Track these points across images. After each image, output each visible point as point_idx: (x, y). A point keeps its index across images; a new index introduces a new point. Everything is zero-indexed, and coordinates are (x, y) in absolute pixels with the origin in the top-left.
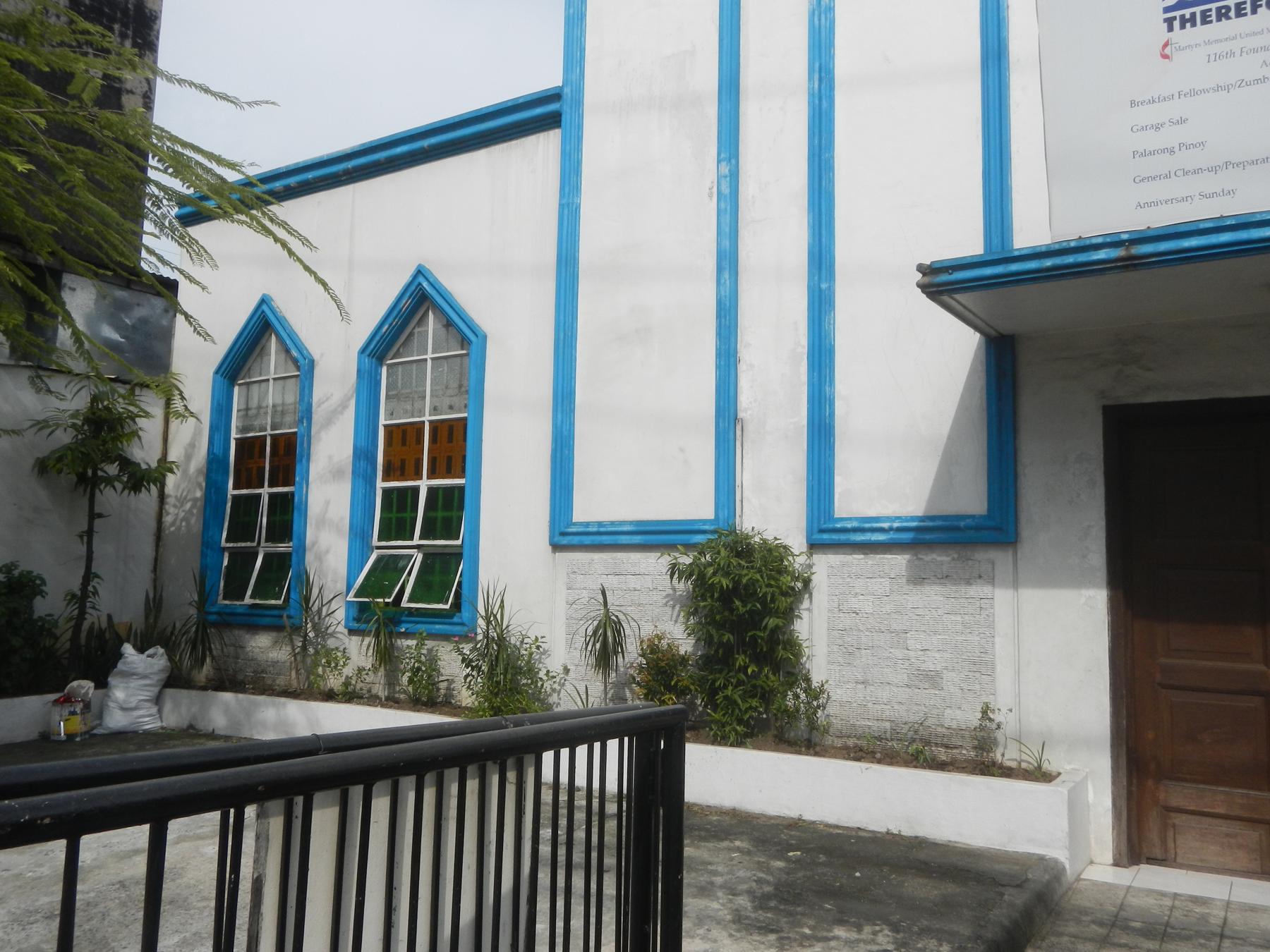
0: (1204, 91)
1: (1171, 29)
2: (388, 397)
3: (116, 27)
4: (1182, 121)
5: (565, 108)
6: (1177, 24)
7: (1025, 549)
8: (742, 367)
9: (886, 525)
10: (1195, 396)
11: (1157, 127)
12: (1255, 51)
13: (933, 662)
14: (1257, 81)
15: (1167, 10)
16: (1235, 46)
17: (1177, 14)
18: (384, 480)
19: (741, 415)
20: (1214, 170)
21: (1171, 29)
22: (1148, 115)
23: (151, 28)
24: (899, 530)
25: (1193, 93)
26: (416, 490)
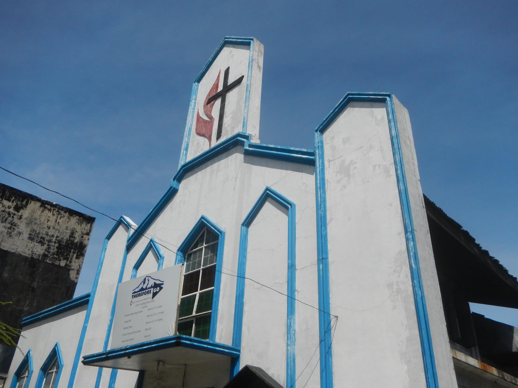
3: (72, 250)
4: (130, 321)
5: (90, 298)
8: (102, 377)
11: (127, 322)
15: (133, 293)
16: (139, 303)
20: (132, 333)
22: (128, 318)
25: (133, 314)
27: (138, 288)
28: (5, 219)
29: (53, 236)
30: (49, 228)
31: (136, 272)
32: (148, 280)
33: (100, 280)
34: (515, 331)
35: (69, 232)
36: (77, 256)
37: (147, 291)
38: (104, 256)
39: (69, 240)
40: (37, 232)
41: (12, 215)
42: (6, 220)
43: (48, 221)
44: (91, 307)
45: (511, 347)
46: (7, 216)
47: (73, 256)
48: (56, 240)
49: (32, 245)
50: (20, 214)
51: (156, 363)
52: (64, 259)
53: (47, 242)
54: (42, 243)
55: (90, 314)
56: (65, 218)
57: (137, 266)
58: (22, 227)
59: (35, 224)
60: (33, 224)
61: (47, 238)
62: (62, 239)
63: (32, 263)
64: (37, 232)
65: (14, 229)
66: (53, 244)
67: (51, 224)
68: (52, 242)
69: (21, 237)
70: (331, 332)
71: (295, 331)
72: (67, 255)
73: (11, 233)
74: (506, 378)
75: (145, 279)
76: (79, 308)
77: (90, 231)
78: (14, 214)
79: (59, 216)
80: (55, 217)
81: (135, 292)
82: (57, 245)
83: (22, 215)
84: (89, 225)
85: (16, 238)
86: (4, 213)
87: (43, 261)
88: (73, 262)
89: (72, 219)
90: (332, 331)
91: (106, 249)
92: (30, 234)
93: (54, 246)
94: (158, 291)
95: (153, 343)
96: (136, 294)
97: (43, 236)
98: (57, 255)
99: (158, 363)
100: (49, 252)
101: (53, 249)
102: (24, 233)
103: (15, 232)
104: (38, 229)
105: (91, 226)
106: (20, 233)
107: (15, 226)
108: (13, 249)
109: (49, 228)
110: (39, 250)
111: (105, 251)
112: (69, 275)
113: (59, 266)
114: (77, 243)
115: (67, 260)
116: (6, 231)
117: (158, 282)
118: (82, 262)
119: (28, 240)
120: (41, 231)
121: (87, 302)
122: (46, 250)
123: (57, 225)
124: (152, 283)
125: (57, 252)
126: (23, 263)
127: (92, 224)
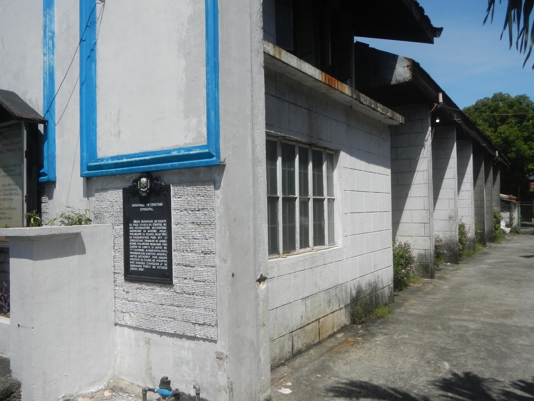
34: (399, 60)
45: (391, 79)
70: (95, 26)
71: (54, 33)
74: (362, 100)
90: (98, 25)
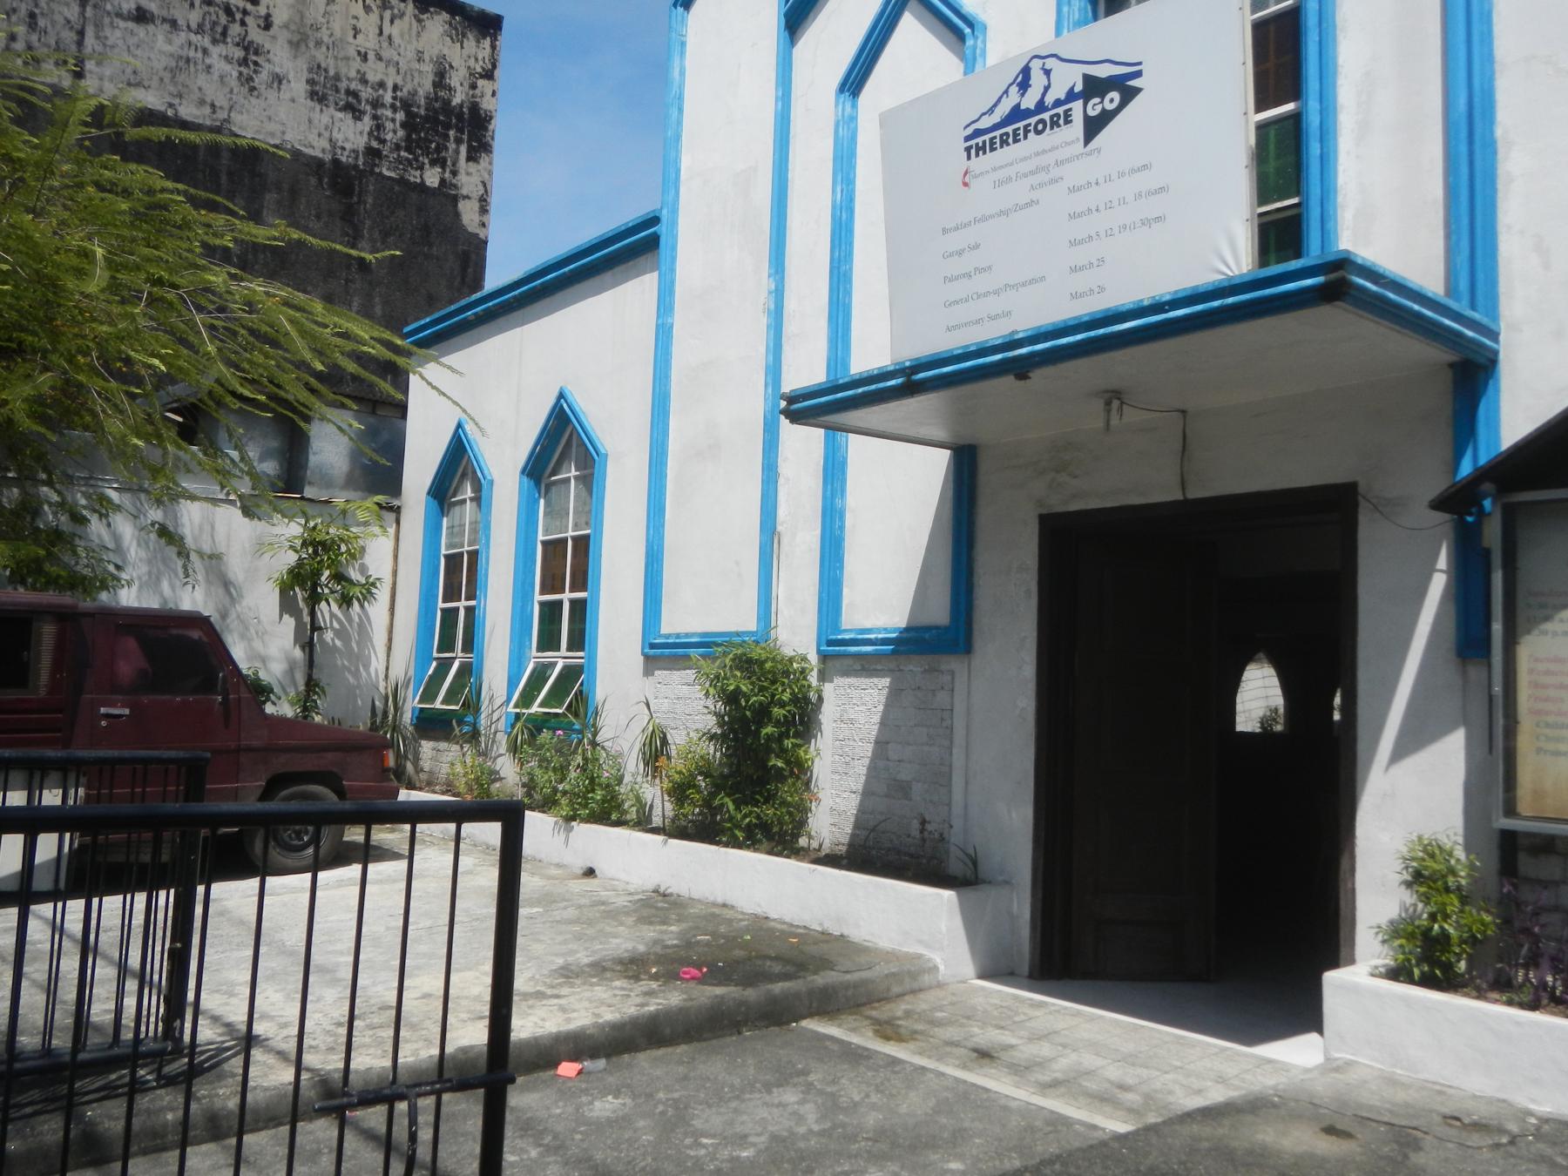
0: (992, 217)
1: (969, 158)
2: (546, 514)
3: (452, 133)
4: (977, 246)
5: (662, 229)
6: (973, 152)
7: (977, 659)
8: (781, 481)
9: (872, 636)
10: (1109, 505)
11: (960, 253)
12: (1025, 176)
13: (905, 774)
14: (1028, 205)
15: (967, 139)
16: (1011, 171)
17: (973, 142)
18: (542, 592)
19: (779, 528)
20: (996, 292)
21: (969, 158)
23: (486, 129)
24: (885, 642)
25: (984, 219)
26: (560, 603)
27: (991, 110)
28: (219, 29)
29: (382, 85)
30: (365, 58)
31: (854, 106)
32: (1047, 73)
33: (686, 162)
35: (428, 68)
36: (470, 149)
37: (1046, 116)
38: (682, 73)
39: (436, 99)
40: (332, 73)
41: (238, 16)
42: (224, 34)
43: (356, 32)
44: (674, 259)
46: (223, 19)
47: (457, 152)
48: (395, 98)
49: (325, 119)
50: (262, 11)
51: (1099, 404)
52: (433, 163)
53: (368, 108)
54: (352, 108)
55: (673, 282)
56: (406, 18)
57: (854, 82)
58: (280, 56)
59: (318, 43)
60: (311, 45)
61: (366, 93)
62: (414, 93)
63: (340, 180)
64: (332, 73)
65: (256, 63)
66: (389, 113)
67: (368, 41)
68: (383, 105)
69: (285, 95)
72: (438, 150)
73: (252, 79)
75: (1026, 71)
76: (618, 270)
77: (494, 66)
78: (245, 12)
79: (387, 14)
80: (374, 17)
81: (978, 133)
82: (400, 116)
83: (268, 16)
84: (487, 43)
85: (272, 95)
86: (212, 9)
87: (372, 172)
88: (462, 171)
89: (428, 23)
91: (683, 44)
92: (311, 82)
93: (393, 120)
94: (1110, 107)
95: (1175, 303)
96: (980, 141)
97: (354, 86)
98: (408, 149)
99: (1108, 403)
100: (383, 142)
101: (394, 133)
102: (291, 77)
103: (264, 76)
104: (331, 62)
105: (493, 47)
106: (278, 79)
107: (256, 53)
108: (272, 135)
109: (365, 58)
110: (352, 135)
111: (682, 53)
112: (457, 215)
113: (422, 187)
114: (461, 106)
115: (443, 167)
116: (235, 74)
117: (1103, 72)
118: (490, 173)
119: (310, 103)
120: (343, 71)
121: (653, 244)
122: (370, 133)
123: (385, 45)
124: (1067, 78)
125: (408, 138)
126: (313, 181)
127: (494, 39)
